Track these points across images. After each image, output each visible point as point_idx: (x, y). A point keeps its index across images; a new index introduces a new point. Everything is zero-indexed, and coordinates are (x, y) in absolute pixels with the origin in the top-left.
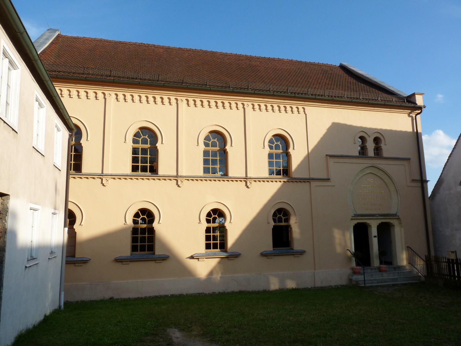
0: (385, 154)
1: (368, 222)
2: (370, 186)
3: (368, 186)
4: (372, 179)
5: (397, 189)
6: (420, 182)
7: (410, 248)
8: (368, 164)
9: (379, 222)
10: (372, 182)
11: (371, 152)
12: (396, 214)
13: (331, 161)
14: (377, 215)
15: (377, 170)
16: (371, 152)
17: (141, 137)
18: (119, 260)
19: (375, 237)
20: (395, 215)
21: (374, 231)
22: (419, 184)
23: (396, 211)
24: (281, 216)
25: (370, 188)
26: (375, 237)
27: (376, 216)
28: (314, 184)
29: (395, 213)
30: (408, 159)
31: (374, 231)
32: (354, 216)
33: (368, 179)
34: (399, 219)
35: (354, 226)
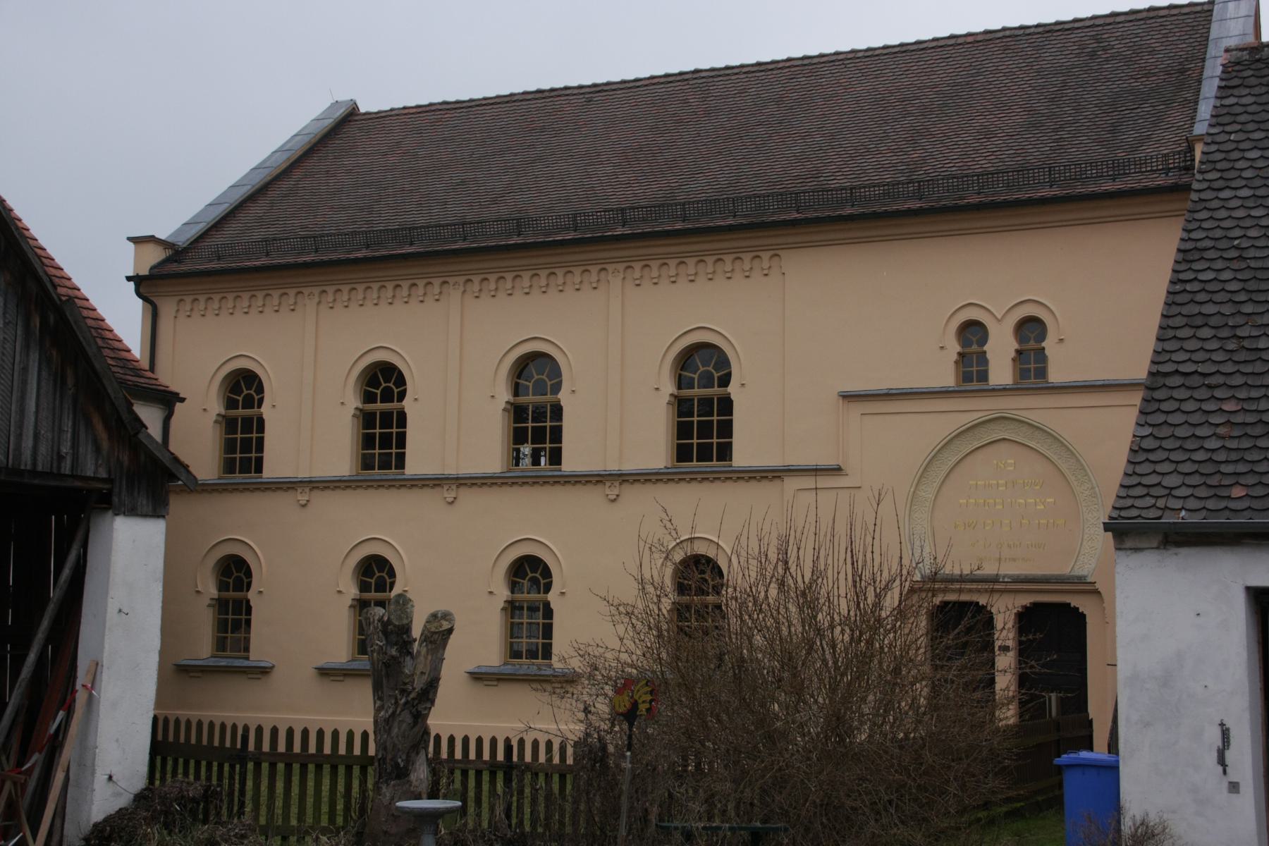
0: (1056, 375)
2: (1000, 482)
4: (1009, 461)
8: (980, 414)
9: (1026, 600)
11: (1001, 371)
13: (858, 408)
14: (1006, 580)
16: (1001, 371)
17: (397, 388)
18: (325, 673)
19: (1005, 649)
21: (1005, 631)
25: (1001, 488)
26: (1005, 649)
27: (1001, 580)
28: (792, 484)
29: (1085, 573)
31: (1005, 631)
34: (1099, 593)
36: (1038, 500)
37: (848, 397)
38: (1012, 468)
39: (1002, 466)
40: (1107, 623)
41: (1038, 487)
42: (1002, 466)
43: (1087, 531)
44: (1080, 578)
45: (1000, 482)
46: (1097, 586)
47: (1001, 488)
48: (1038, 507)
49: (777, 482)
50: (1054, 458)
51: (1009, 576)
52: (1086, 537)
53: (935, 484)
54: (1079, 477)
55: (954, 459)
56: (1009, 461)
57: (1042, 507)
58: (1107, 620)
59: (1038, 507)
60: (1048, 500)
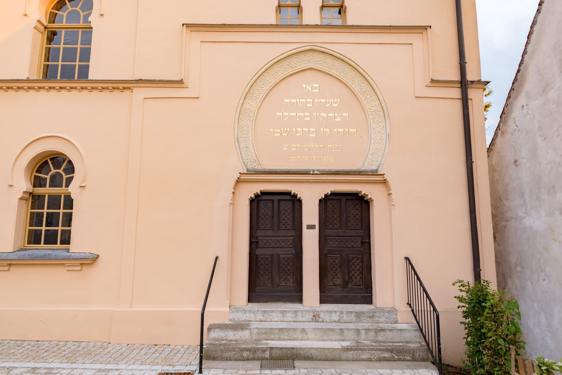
1: (293, 189)
3: (301, 100)
4: (315, 85)
5: (384, 105)
6: (459, 85)
7: (410, 263)
9: (328, 189)
10: (314, 91)
12: (377, 170)
14: (316, 172)
15: (329, 59)
20: (374, 173)
22: (456, 93)
23: (379, 163)
24: (53, 171)
27: (311, 173)
28: (139, 93)
29: (374, 168)
30: (425, 28)
32: (246, 172)
33: (304, 86)
34: (385, 182)
35: (252, 201)
36: (336, 115)
37: (188, 26)
38: (317, 91)
39: (310, 89)
40: (394, 205)
41: (336, 105)
42: (310, 89)
43: (373, 137)
44: (372, 171)
45: (308, 100)
46: (386, 177)
47: (308, 105)
48: (336, 120)
49: (127, 93)
50: (349, 83)
51: (318, 170)
52: (372, 141)
53: (258, 100)
54: (368, 97)
55: (273, 82)
56: (315, 85)
57: (340, 119)
58: (393, 203)
59: (336, 120)
60: (344, 114)
